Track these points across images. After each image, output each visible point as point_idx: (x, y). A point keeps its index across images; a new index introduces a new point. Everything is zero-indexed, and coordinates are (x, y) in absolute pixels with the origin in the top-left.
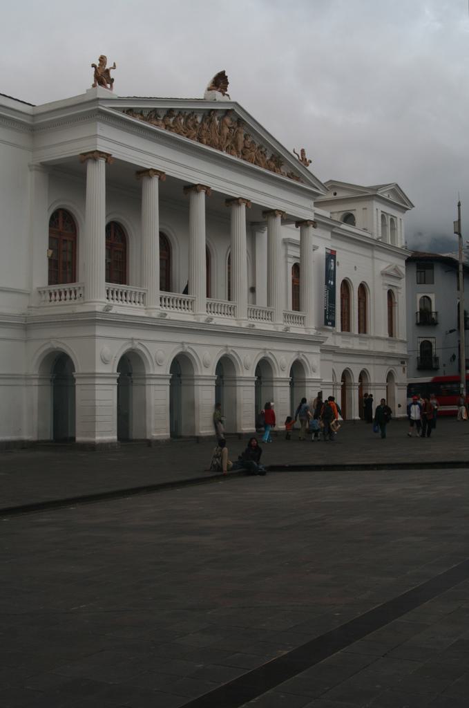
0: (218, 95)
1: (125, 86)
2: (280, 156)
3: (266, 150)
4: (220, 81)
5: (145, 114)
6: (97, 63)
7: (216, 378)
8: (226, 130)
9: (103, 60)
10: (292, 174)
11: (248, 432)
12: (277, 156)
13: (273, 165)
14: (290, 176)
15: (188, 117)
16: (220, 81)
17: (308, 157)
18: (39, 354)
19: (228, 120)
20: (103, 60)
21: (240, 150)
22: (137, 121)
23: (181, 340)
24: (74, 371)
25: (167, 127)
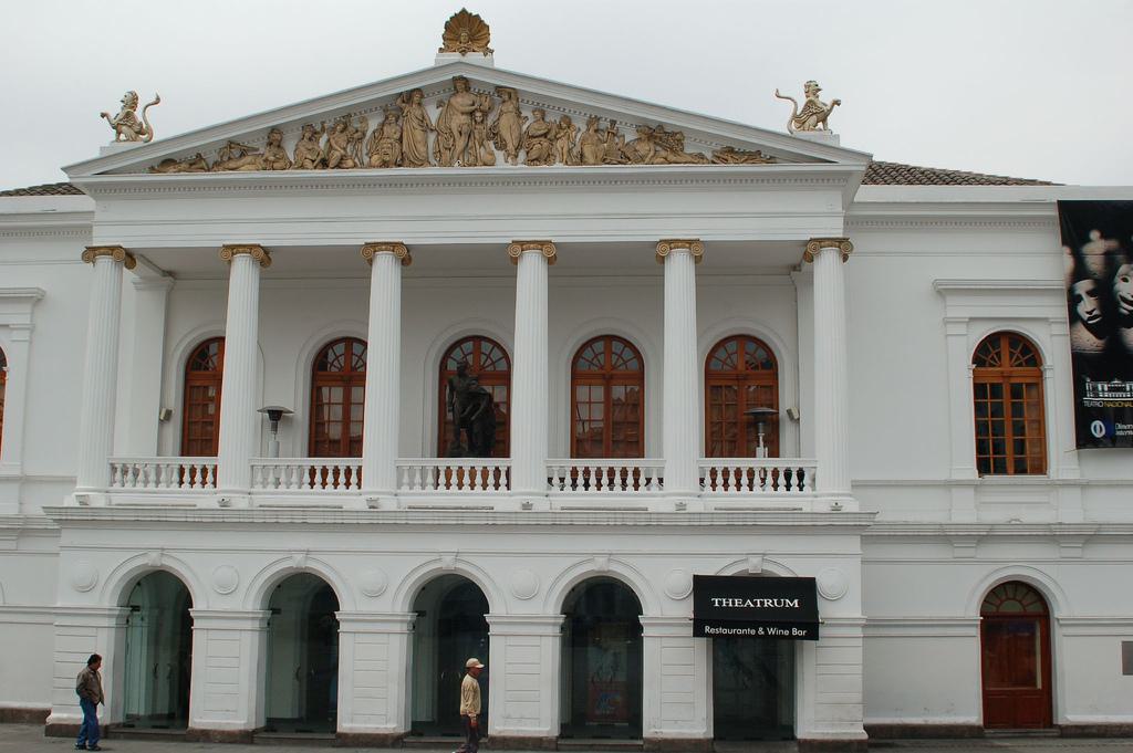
0: (455, 57)
1: (166, 125)
2: (661, 126)
3: (613, 123)
4: (466, 30)
5: (212, 157)
6: (116, 109)
7: (561, 621)
8: (459, 121)
9: (132, 101)
10: (731, 150)
11: (669, 737)
12: (653, 126)
13: (644, 148)
14: (729, 153)
15: (333, 130)
16: (466, 30)
17: (825, 98)
18: (261, 581)
19: (462, 101)
20: (132, 101)
21: (510, 147)
22: (170, 176)
23: (305, 547)
24: (338, 610)
25: (269, 165)
